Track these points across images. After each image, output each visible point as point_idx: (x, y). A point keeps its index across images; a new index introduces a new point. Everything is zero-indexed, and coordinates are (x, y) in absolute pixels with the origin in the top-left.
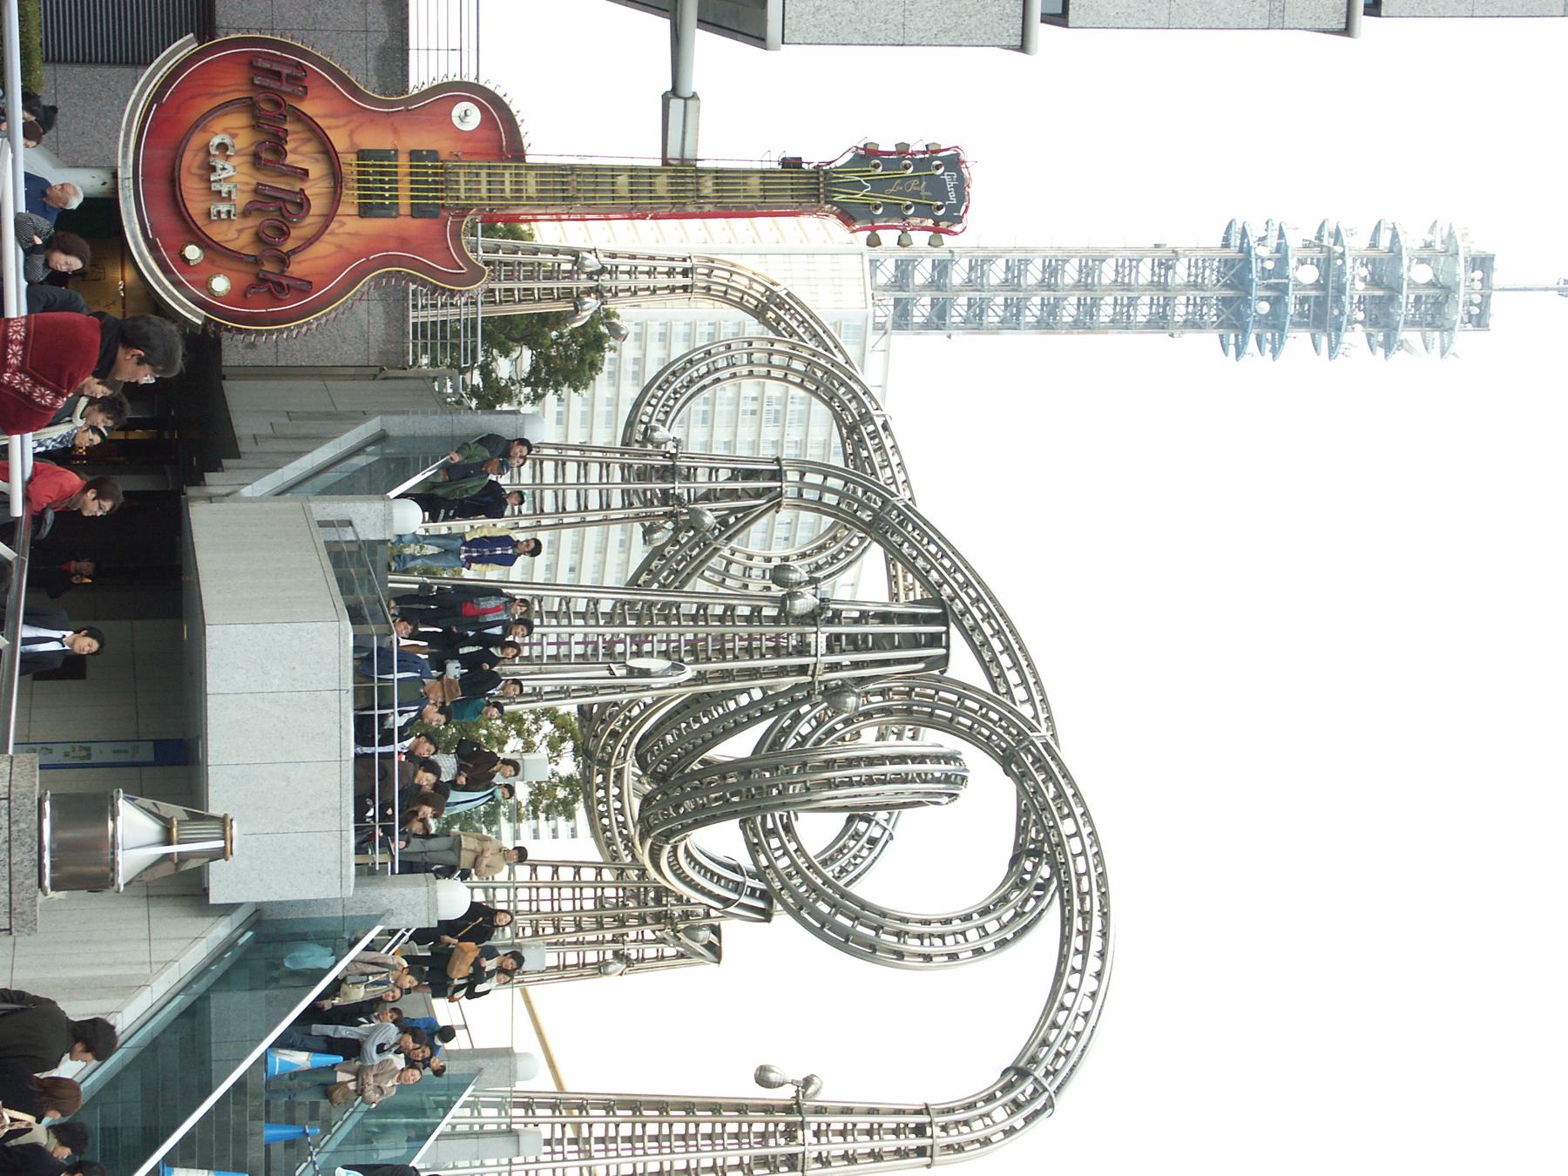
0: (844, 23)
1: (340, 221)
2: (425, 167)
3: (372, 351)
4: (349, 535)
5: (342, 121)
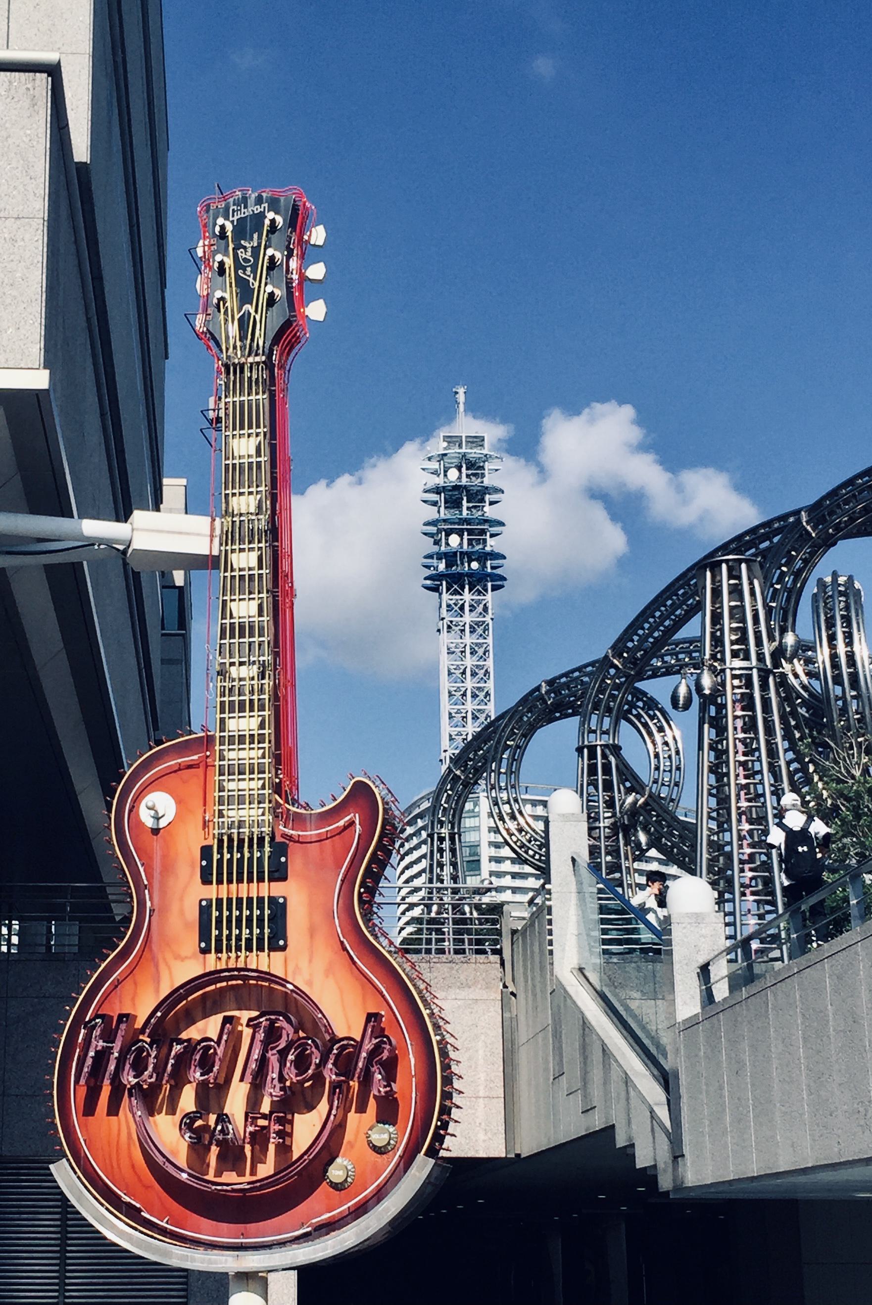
0: (14, 293)
1: (294, 973)
2: (220, 861)
3: (485, 997)
4: (720, 970)
5: (162, 967)
